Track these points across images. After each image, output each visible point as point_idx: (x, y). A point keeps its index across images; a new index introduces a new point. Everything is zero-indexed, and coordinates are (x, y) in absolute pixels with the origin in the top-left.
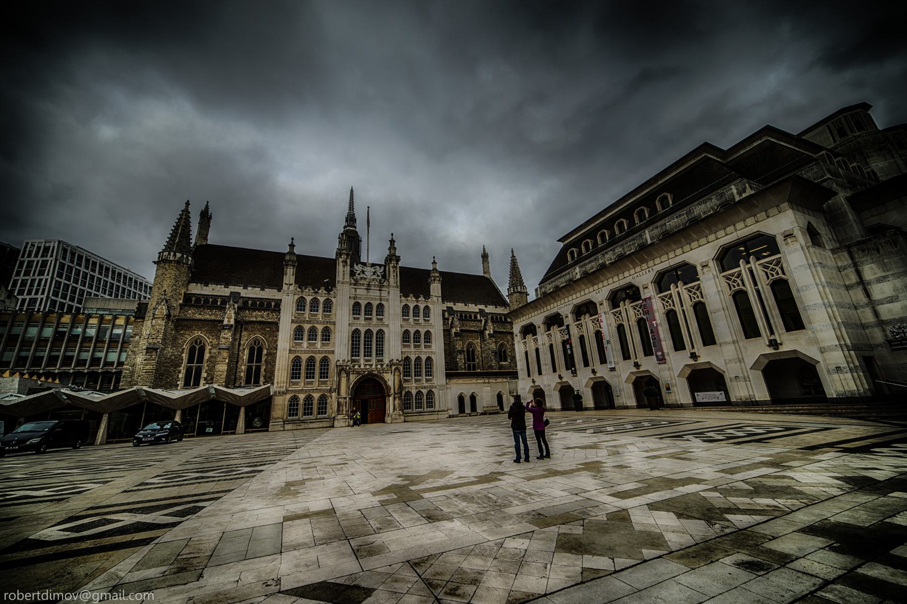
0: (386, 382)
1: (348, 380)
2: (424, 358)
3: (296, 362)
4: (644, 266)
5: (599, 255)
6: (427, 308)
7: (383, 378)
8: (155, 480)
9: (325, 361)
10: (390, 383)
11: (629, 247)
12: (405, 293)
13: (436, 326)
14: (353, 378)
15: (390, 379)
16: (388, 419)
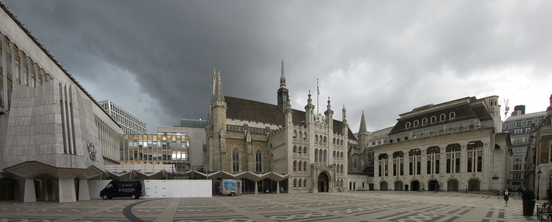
0: (329, 175)
1: (317, 173)
2: (340, 165)
3: (295, 163)
4: (444, 141)
5: (423, 129)
6: (342, 140)
7: (328, 173)
8: (109, 211)
9: (305, 163)
10: (331, 175)
11: (435, 129)
12: (334, 133)
13: (345, 150)
14: (319, 172)
15: (331, 173)
16: (330, 190)
